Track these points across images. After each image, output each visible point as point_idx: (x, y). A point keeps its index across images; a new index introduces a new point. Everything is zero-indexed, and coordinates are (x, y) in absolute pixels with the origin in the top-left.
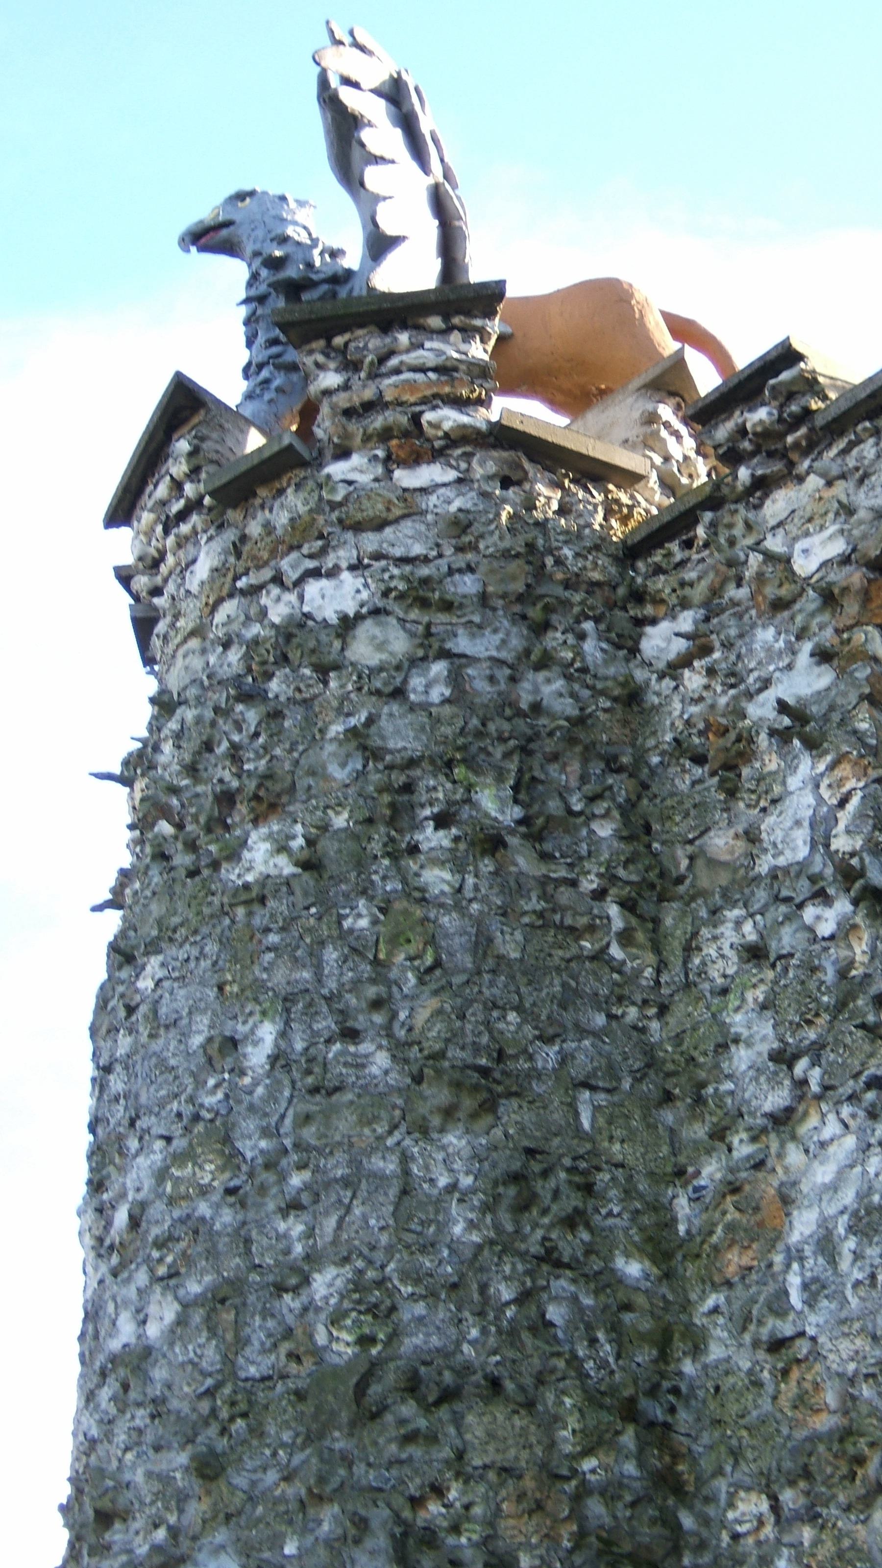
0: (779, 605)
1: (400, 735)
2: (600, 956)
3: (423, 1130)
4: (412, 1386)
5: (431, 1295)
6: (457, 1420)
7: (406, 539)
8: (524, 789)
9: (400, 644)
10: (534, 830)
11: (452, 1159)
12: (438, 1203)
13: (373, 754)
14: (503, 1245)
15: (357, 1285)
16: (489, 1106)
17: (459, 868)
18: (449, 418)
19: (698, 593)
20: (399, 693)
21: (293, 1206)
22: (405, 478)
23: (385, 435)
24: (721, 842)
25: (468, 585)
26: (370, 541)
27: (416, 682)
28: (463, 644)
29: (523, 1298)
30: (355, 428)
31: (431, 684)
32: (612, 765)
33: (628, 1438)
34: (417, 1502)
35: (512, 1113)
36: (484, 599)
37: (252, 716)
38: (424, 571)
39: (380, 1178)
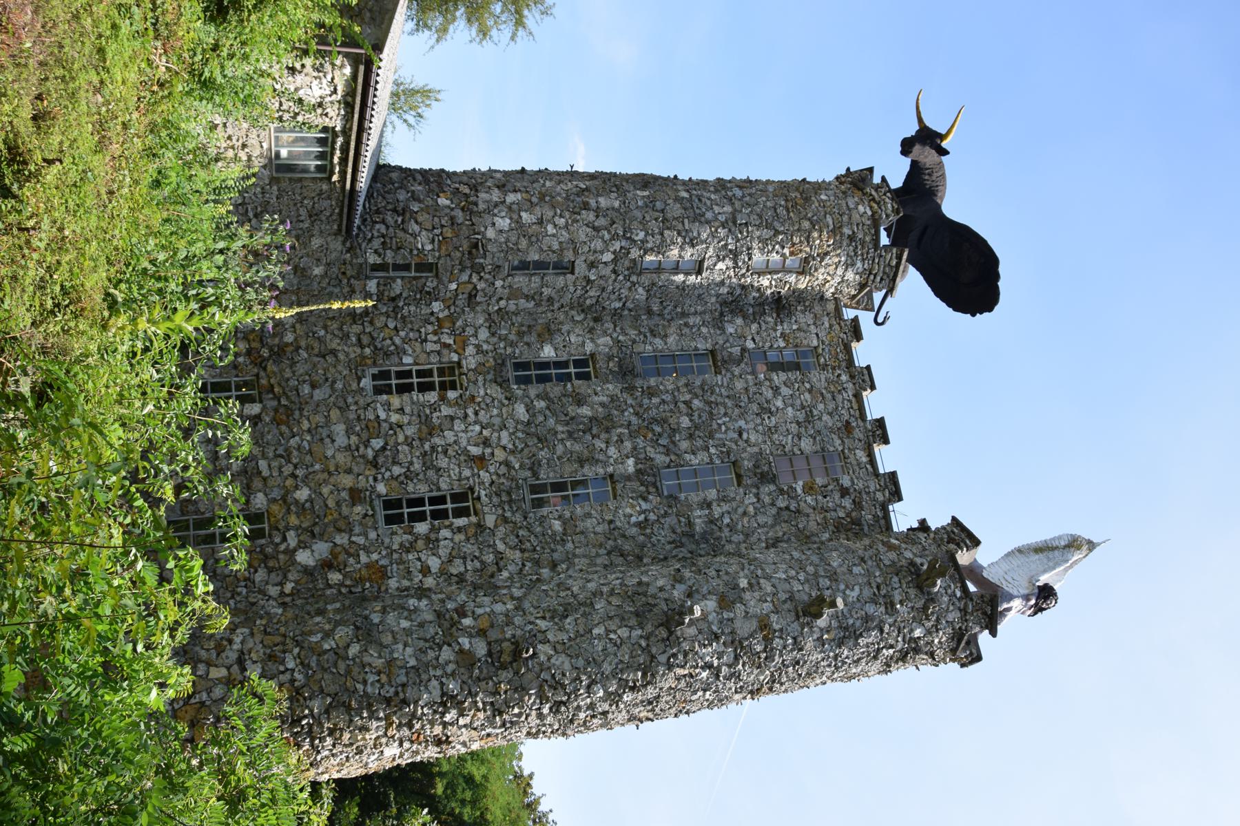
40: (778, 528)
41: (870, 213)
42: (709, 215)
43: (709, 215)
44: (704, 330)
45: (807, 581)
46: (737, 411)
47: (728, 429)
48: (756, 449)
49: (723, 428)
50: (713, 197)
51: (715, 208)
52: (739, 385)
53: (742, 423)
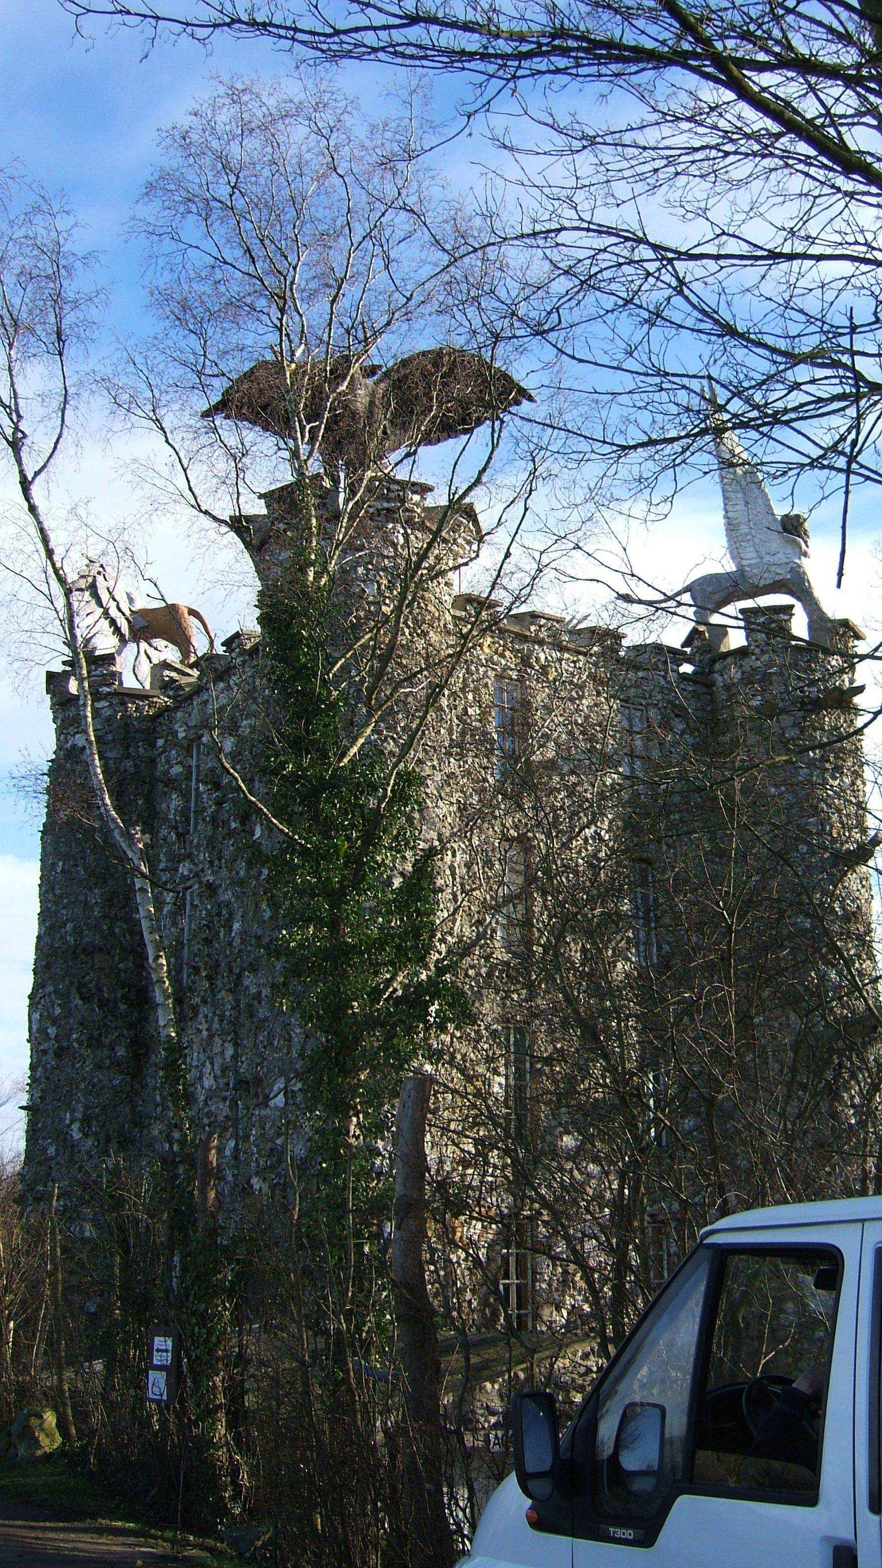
3: (90, 889)
4: (84, 950)
5: (89, 929)
6: (92, 959)
11: (95, 897)
12: (92, 907)
14: (105, 917)
15: (75, 928)
16: (105, 881)
21: (64, 908)
24: (164, 806)
29: (109, 928)
33: (131, 958)
34: (83, 977)
35: (110, 882)
39: (80, 901)
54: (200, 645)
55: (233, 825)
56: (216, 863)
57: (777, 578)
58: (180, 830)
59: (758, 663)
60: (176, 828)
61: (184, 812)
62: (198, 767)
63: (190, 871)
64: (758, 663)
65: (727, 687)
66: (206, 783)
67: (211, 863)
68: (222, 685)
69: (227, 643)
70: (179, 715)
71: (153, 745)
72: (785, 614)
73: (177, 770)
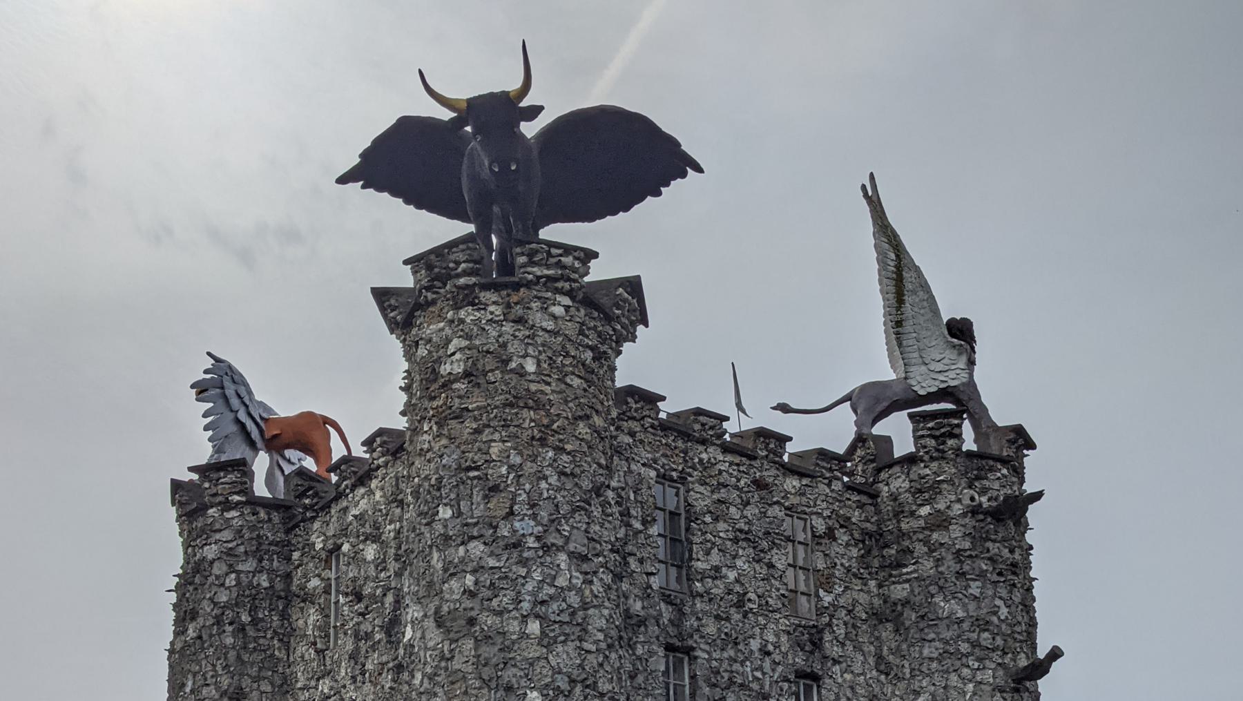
0: (313, 557)
1: (223, 598)
2: (272, 655)
7: (226, 535)
8: (253, 610)
9: (225, 568)
10: (255, 622)
13: (215, 604)
17: (234, 637)
18: (236, 498)
19: (300, 546)
20: (223, 585)
22: (228, 515)
23: (220, 503)
24: (301, 622)
25: (242, 549)
26: (218, 536)
27: (227, 581)
28: (240, 567)
30: (212, 500)
31: (231, 580)
32: (280, 597)
36: (246, 552)
37: (191, 588)
38: (230, 545)
40: (866, 649)
41: (567, 301)
42: (574, 599)
43: (574, 599)
44: (640, 651)
45: (979, 660)
46: (741, 647)
47: (760, 668)
48: (784, 638)
49: (759, 674)
50: (537, 576)
51: (561, 582)
52: (711, 628)
53: (755, 644)
54: (338, 451)
55: (377, 637)
56: (359, 678)
57: (943, 386)
58: (319, 646)
59: (927, 471)
60: (315, 644)
61: (324, 629)
62: (337, 579)
63: (331, 688)
64: (927, 471)
65: (894, 497)
66: (347, 594)
67: (354, 678)
68: (362, 490)
69: (369, 443)
70: (317, 525)
71: (288, 559)
72: (955, 418)
73: (315, 582)
